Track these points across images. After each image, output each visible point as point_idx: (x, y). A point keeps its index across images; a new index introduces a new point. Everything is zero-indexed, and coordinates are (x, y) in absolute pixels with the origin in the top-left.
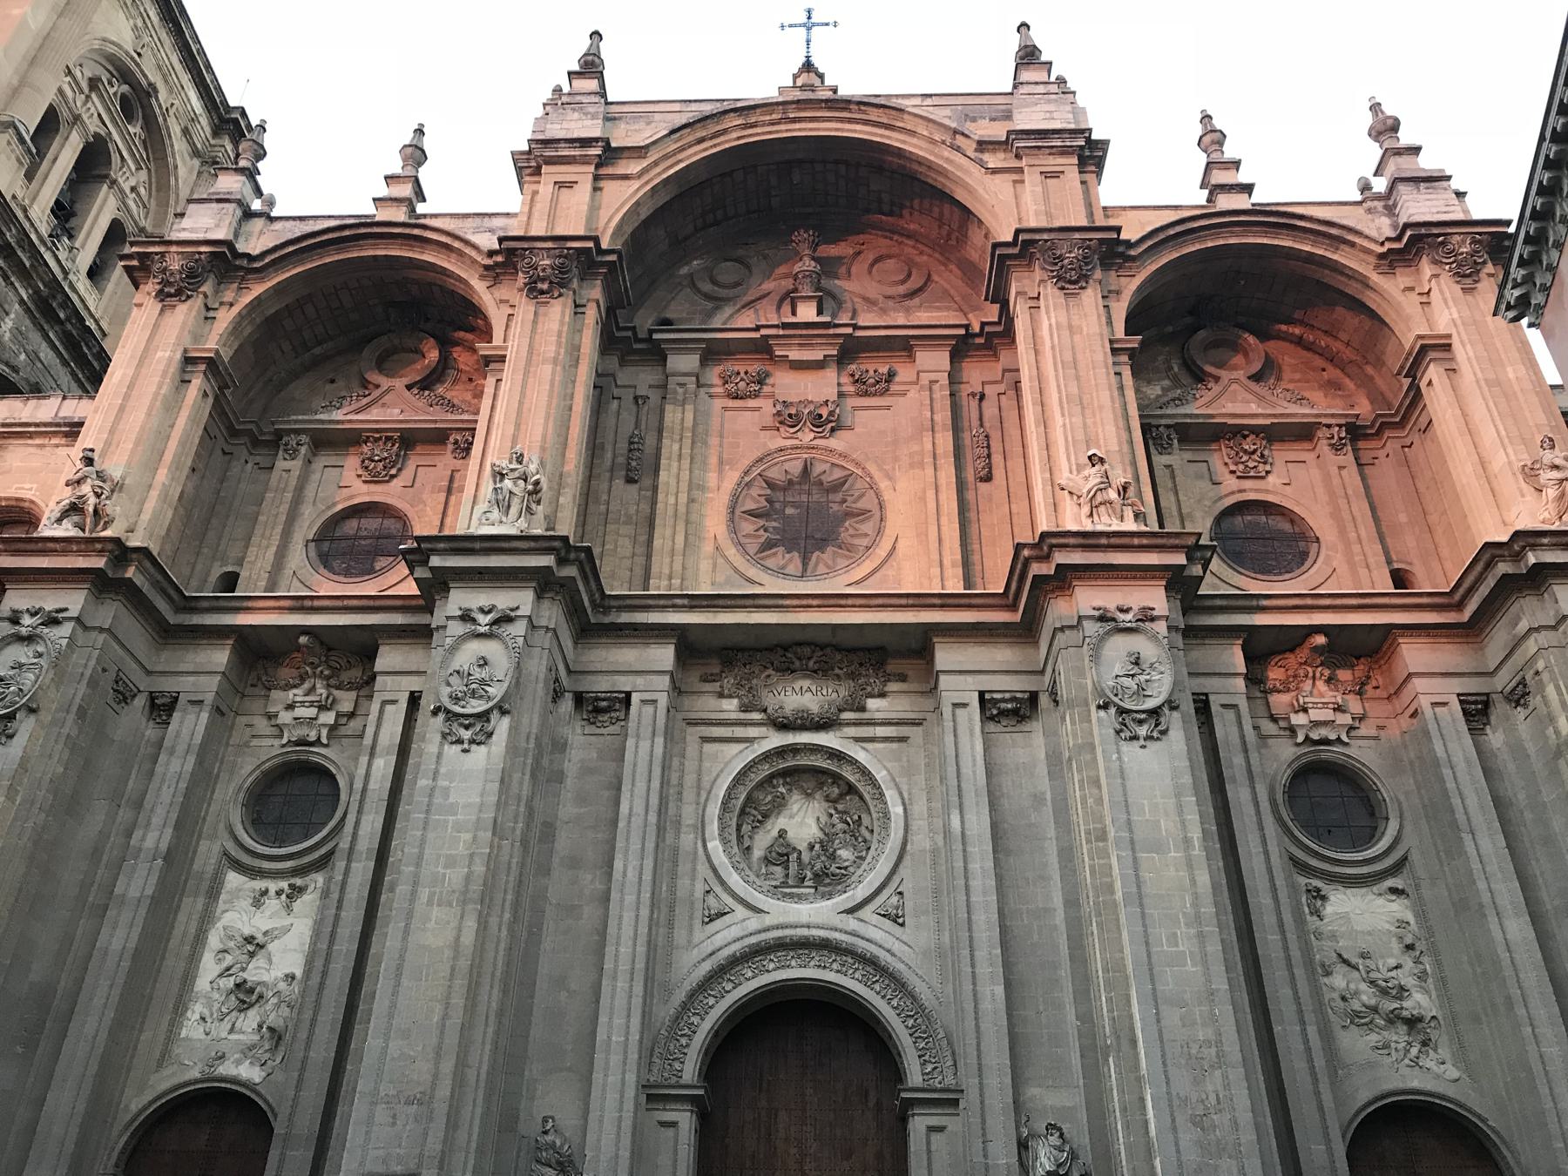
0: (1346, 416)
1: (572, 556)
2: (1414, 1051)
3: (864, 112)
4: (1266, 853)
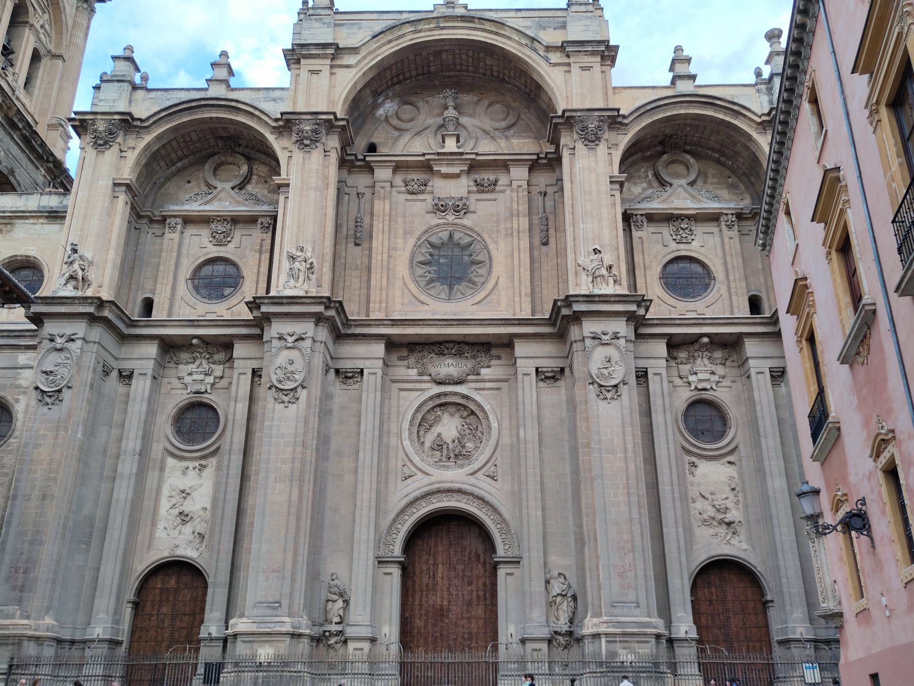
0: (736, 209)
1: (332, 305)
2: (729, 537)
3: (482, 24)
4: (668, 449)
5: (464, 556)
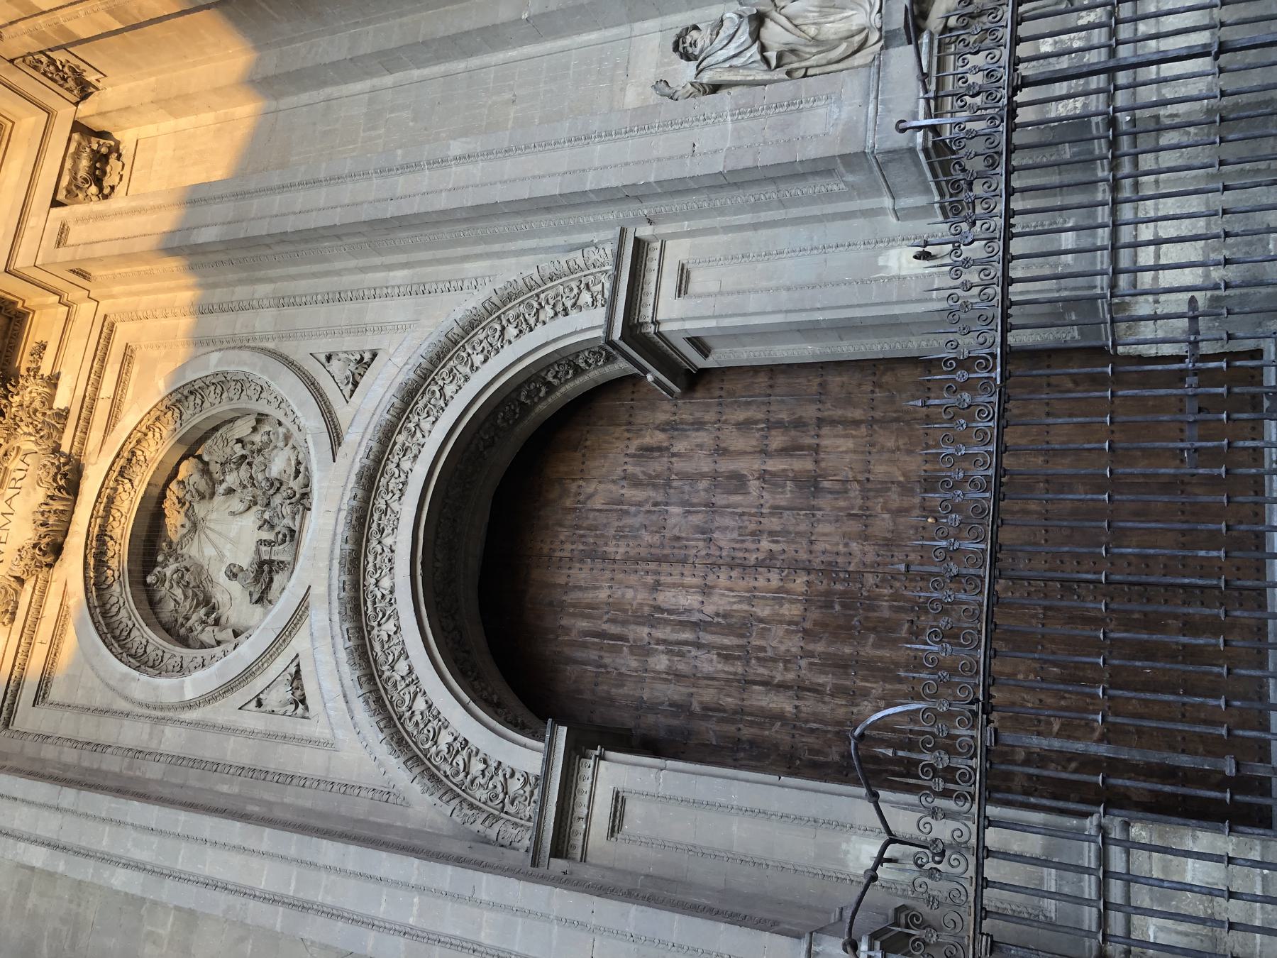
5: (640, 504)
